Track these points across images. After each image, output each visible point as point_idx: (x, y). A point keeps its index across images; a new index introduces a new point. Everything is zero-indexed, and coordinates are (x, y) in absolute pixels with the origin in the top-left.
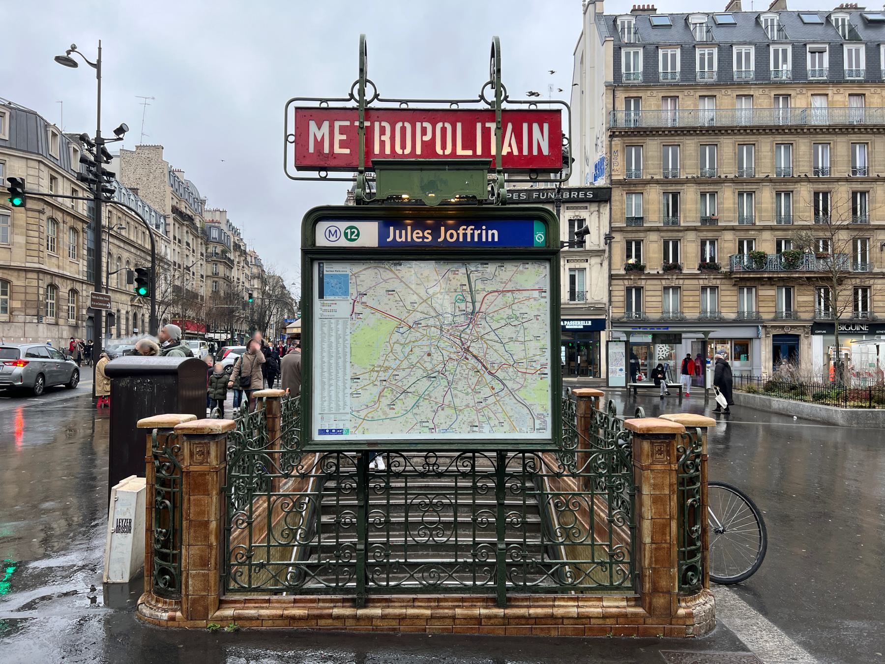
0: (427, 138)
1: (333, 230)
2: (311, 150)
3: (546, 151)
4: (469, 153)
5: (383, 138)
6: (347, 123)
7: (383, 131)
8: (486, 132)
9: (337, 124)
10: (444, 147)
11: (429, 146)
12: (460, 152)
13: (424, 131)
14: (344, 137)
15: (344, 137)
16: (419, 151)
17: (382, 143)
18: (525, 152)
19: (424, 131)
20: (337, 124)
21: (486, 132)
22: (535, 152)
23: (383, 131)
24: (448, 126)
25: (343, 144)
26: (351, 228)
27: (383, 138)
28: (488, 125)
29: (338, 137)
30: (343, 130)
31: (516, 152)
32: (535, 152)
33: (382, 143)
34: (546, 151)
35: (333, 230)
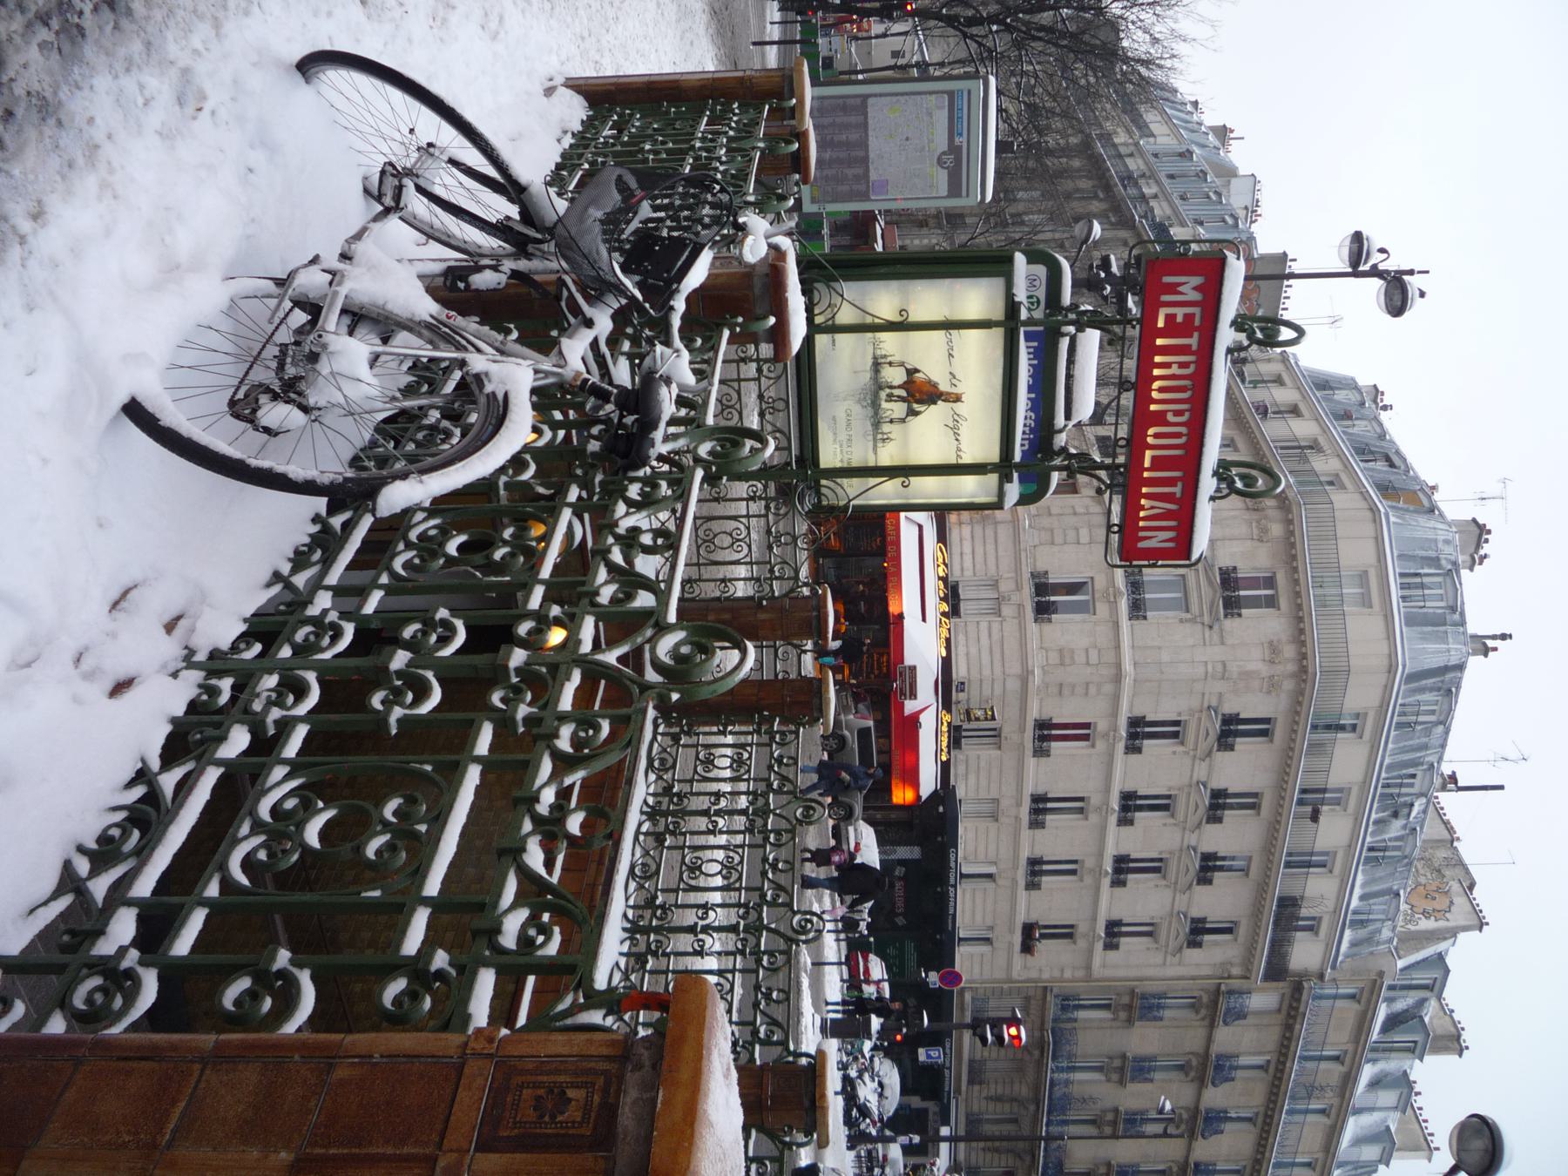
0: (1170, 418)
1: (1037, 283)
2: (1167, 279)
3: (1141, 545)
4: (1147, 464)
5: (1175, 366)
6: (1197, 322)
7: (1182, 365)
8: (1170, 482)
9: (1196, 311)
10: (1156, 436)
11: (1160, 418)
12: (1148, 454)
13: (1178, 413)
14: (1179, 319)
15: (1179, 319)
16: (1153, 407)
17: (1167, 365)
18: (1141, 524)
19: (1178, 413)
20: (1196, 311)
21: (1170, 482)
22: (1142, 534)
23: (1182, 365)
24: (1182, 441)
25: (1170, 318)
26: (1038, 302)
27: (1175, 366)
28: (1180, 484)
29: (1180, 313)
30: (1189, 318)
31: (1142, 514)
32: (1142, 534)
33: (1167, 365)
34: (1141, 545)
35: (1037, 283)
